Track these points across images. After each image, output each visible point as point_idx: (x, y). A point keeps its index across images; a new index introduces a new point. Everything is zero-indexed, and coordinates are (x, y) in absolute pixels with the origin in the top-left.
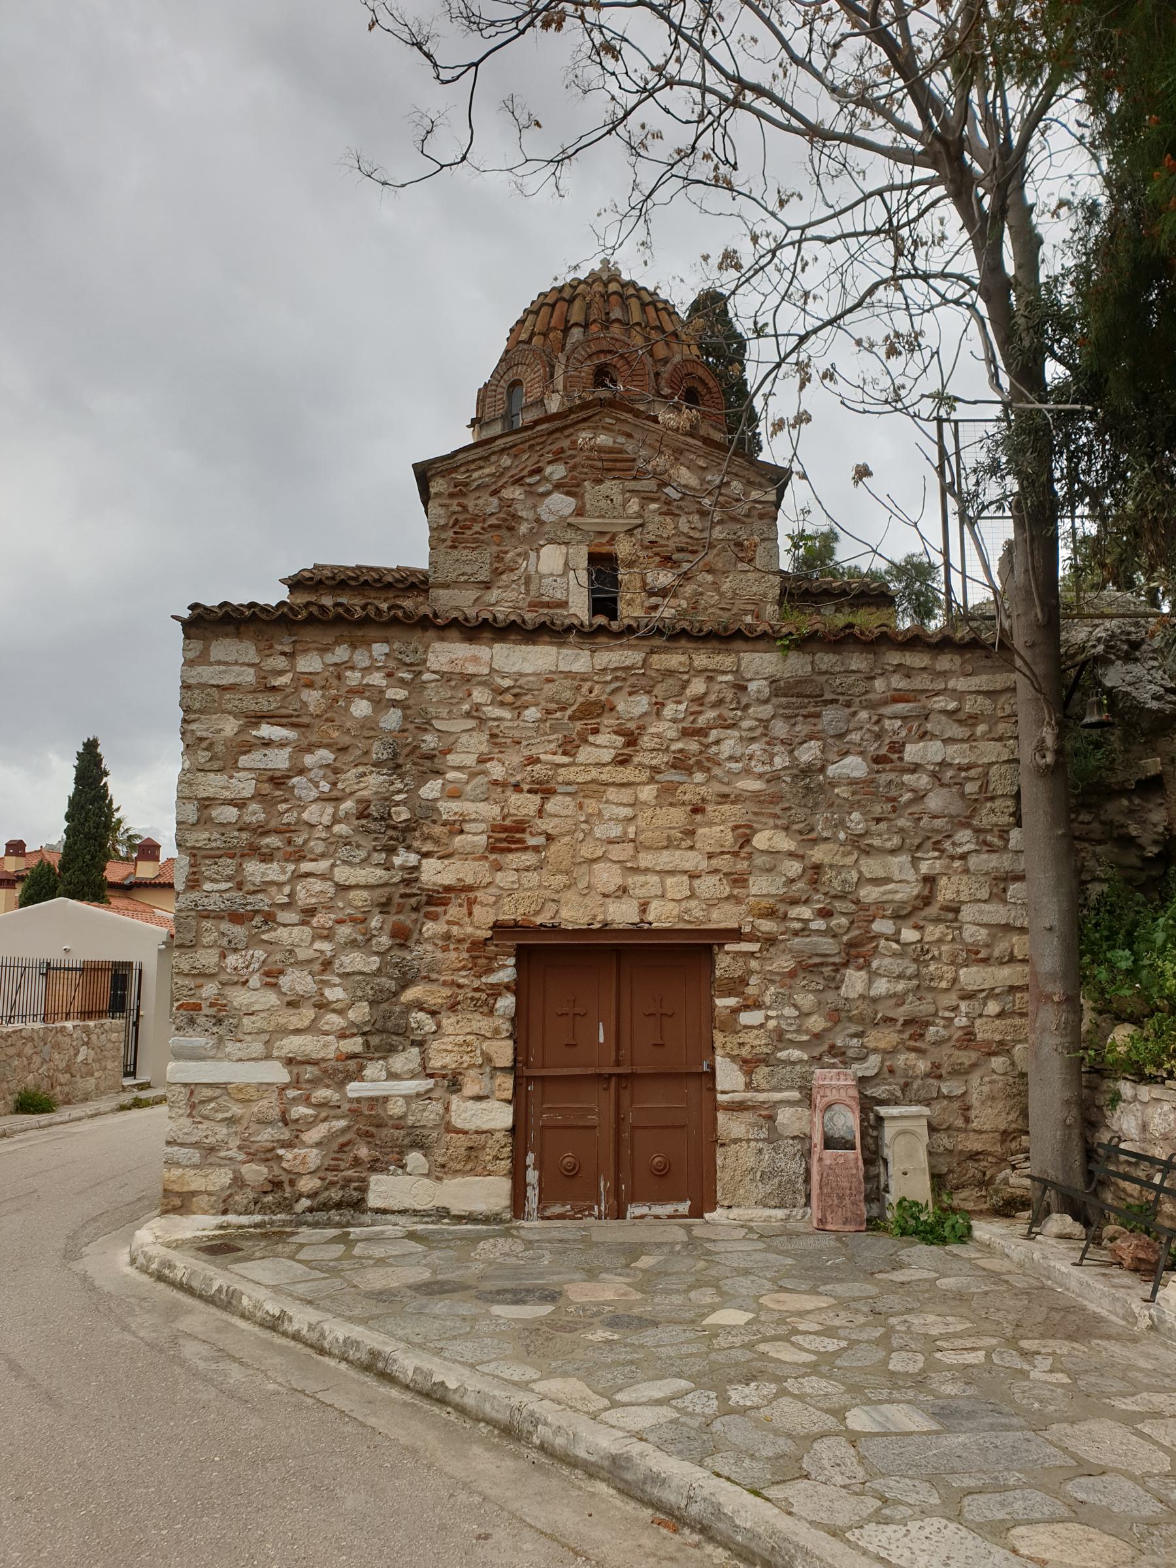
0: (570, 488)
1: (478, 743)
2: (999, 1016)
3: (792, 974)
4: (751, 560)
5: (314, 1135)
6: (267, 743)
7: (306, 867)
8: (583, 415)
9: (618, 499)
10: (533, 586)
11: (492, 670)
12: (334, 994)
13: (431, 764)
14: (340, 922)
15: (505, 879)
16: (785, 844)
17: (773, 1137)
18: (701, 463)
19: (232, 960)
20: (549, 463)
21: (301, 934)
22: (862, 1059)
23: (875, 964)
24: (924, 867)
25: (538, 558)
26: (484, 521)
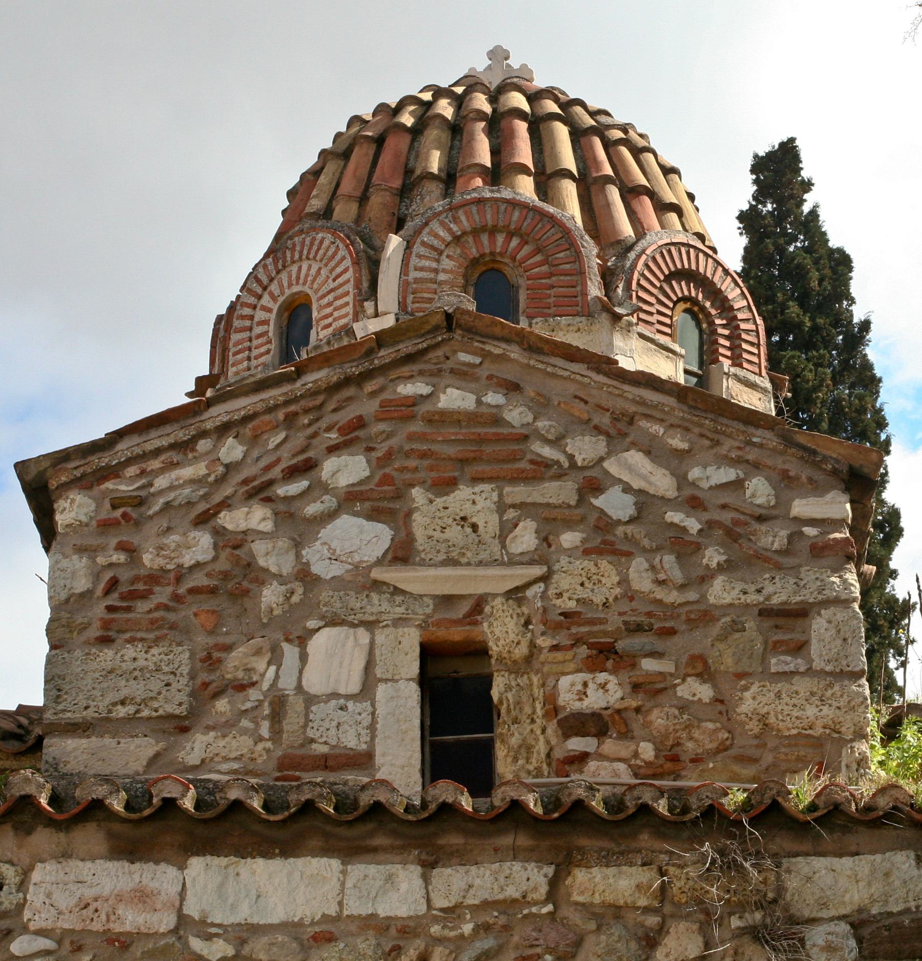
4: (800, 648)
8: (406, 347)
9: (488, 522)
10: (291, 722)
11: (183, 920)
18: (678, 442)
20: (333, 450)
25: (304, 658)
26: (179, 579)
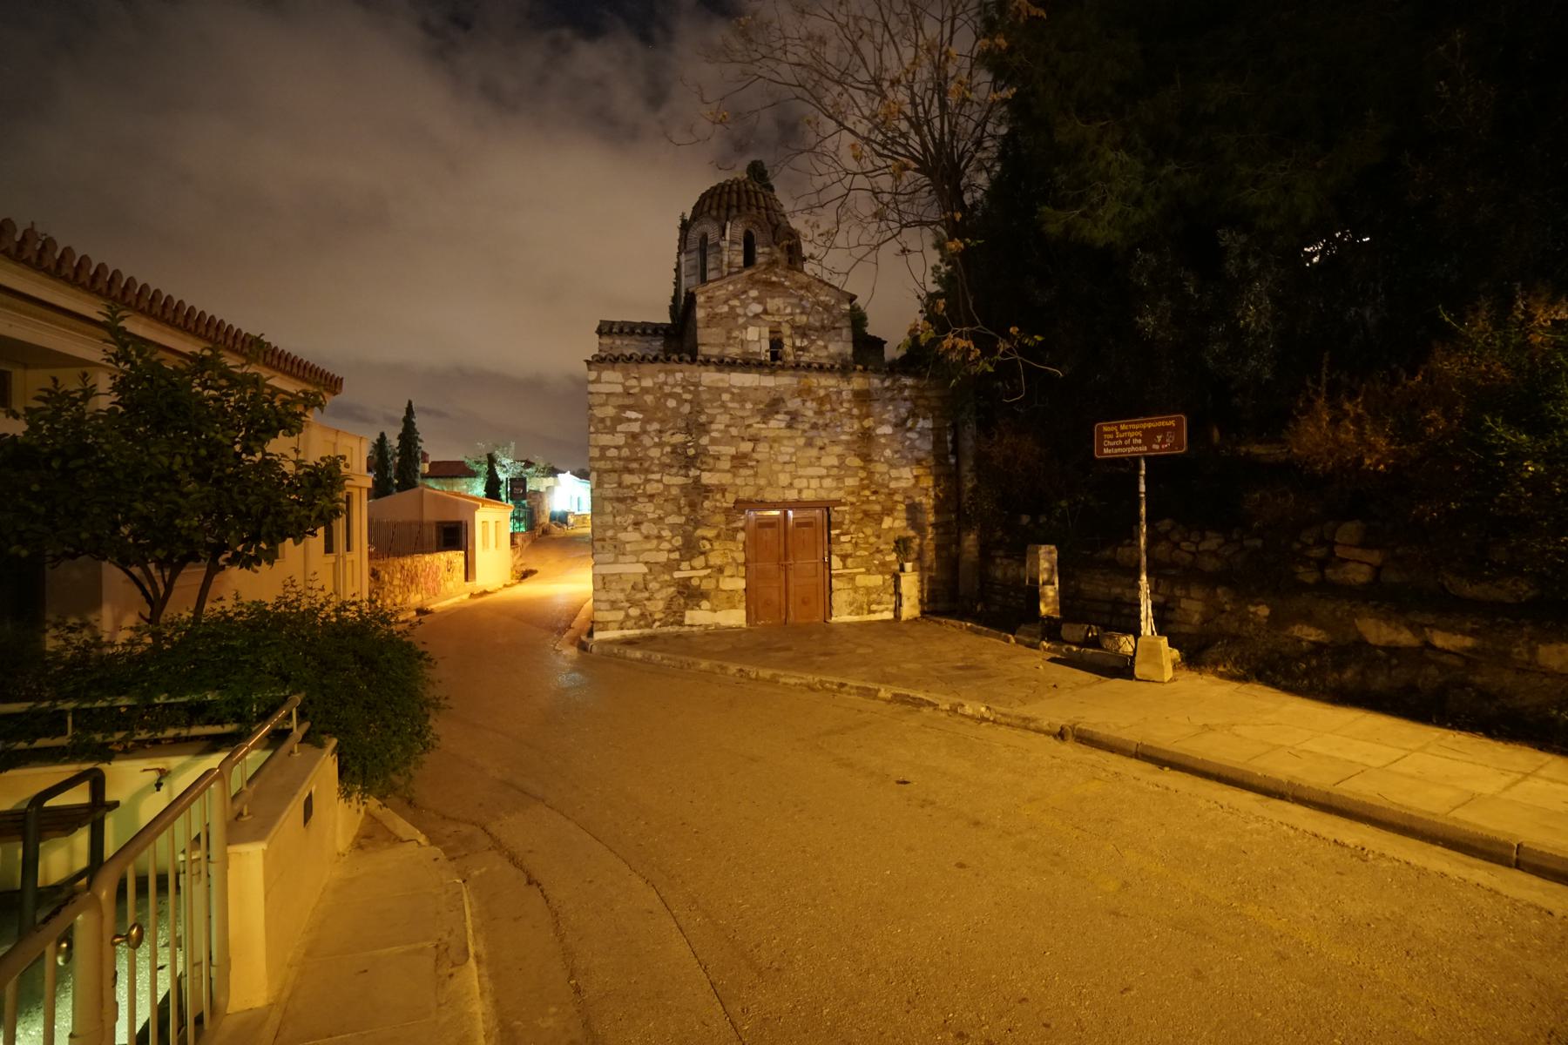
0: (758, 300)
1: (725, 419)
5: (658, 596)
6: (629, 420)
12: (666, 533)
13: (703, 429)
15: (739, 481)
16: (857, 462)
17: (856, 589)
21: (650, 507)
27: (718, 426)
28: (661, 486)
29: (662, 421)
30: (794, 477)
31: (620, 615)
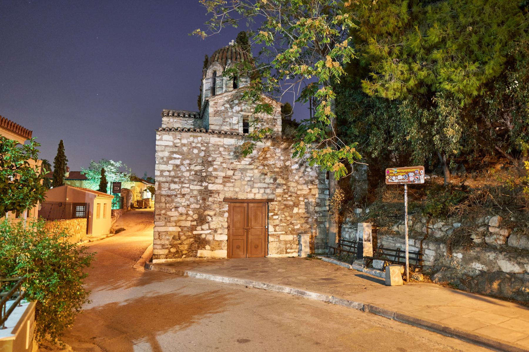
2: (323, 216)
3: (284, 208)
5: (185, 242)
6: (175, 158)
7: (184, 185)
12: (191, 213)
13: (210, 163)
14: (191, 197)
15: (226, 189)
17: (280, 241)
19: (167, 205)
22: (296, 225)
23: (300, 206)
24: (309, 187)
27: (217, 163)
28: (189, 190)
29: (191, 159)
30: (252, 187)
31: (166, 251)
